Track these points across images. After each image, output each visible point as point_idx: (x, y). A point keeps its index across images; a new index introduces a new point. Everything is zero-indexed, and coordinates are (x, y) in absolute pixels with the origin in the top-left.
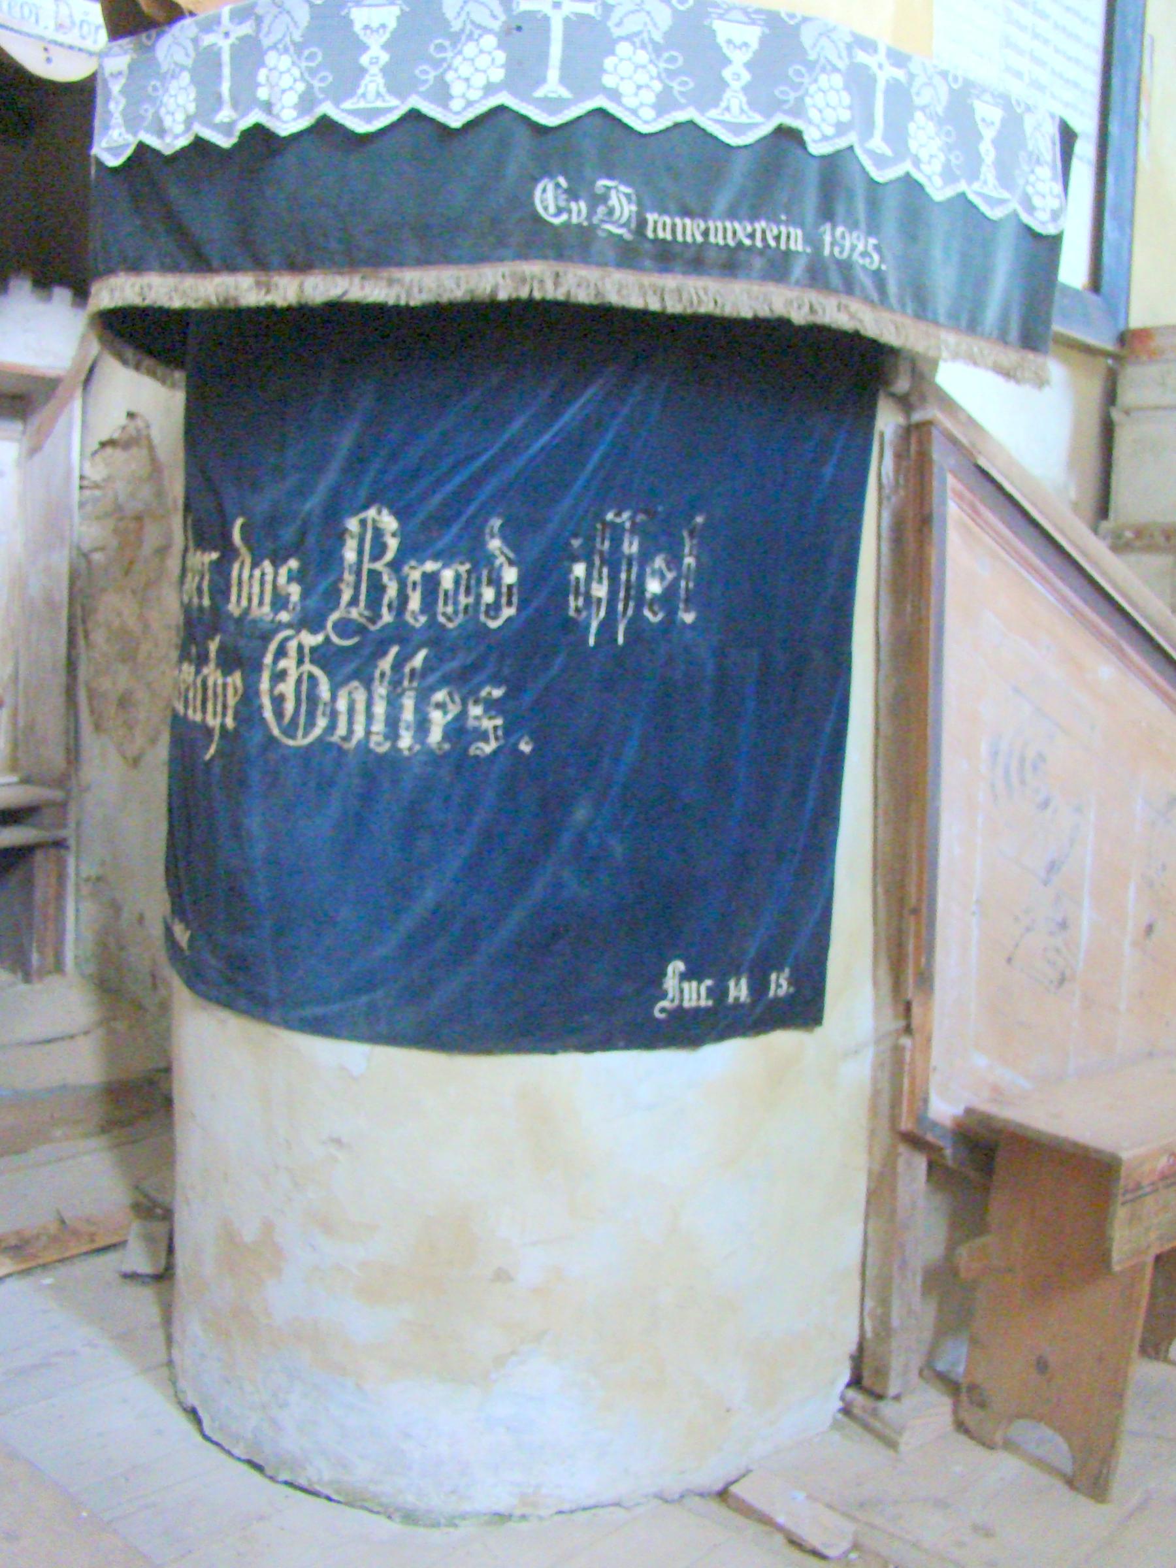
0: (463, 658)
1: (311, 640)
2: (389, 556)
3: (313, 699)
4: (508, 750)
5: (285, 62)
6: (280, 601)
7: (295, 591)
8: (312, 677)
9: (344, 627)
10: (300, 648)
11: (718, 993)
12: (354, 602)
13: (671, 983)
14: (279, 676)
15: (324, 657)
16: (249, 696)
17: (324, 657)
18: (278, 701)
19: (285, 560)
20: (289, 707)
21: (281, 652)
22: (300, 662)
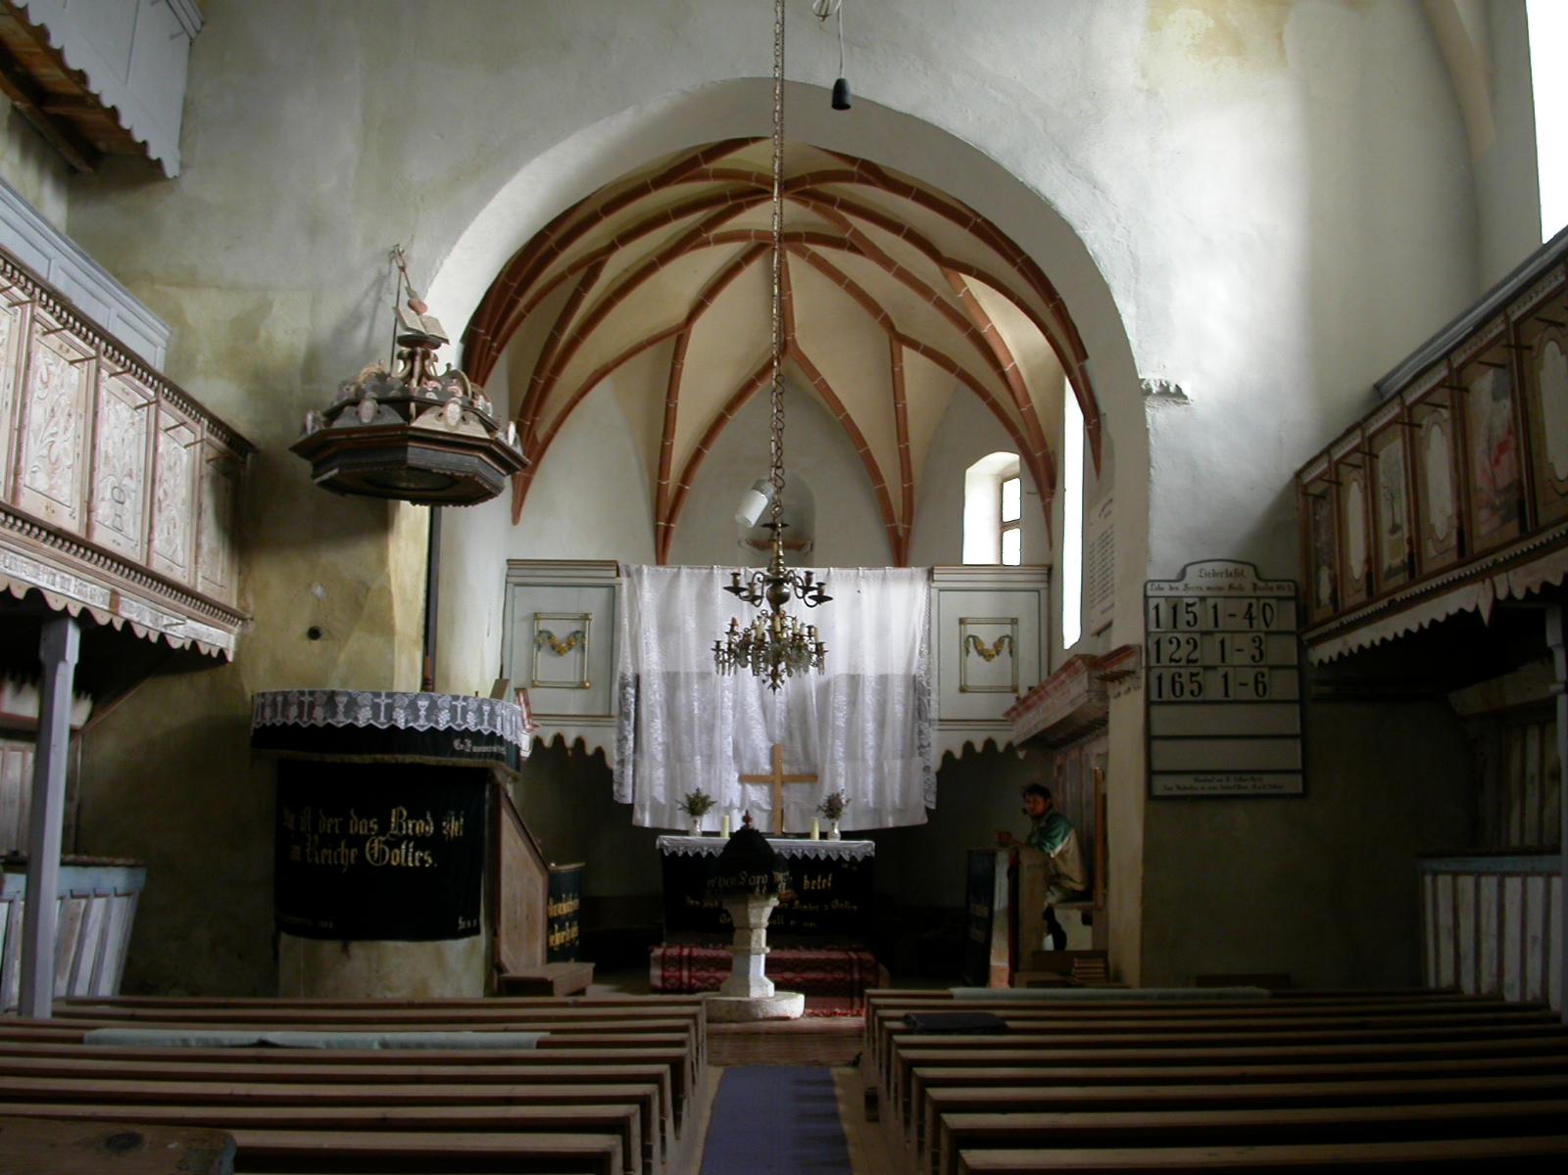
0: (421, 842)
1: (382, 839)
2: (404, 818)
3: (384, 852)
4: (432, 865)
5: (402, 711)
6: (370, 829)
7: (376, 827)
8: (383, 849)
9: (392, 835)
10: (379, 841)
11: (466, 925)
12: (395, 829)
13: (460, 922)
14: (372, 849)
15: (385, 843)
16: (361, 855)
17: (386, 843)
18: (372, 855)
19: (371, 818)
20: (376, 855)
21: (373, 842)
22: (379, 844)
